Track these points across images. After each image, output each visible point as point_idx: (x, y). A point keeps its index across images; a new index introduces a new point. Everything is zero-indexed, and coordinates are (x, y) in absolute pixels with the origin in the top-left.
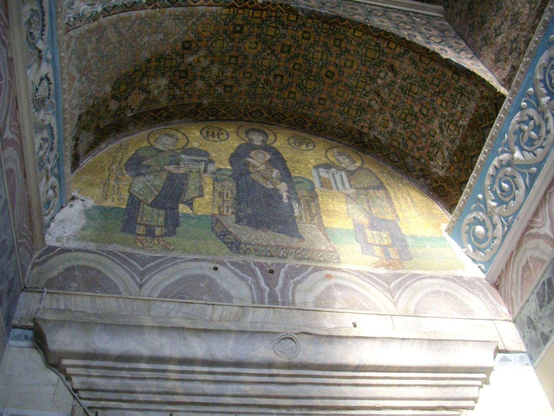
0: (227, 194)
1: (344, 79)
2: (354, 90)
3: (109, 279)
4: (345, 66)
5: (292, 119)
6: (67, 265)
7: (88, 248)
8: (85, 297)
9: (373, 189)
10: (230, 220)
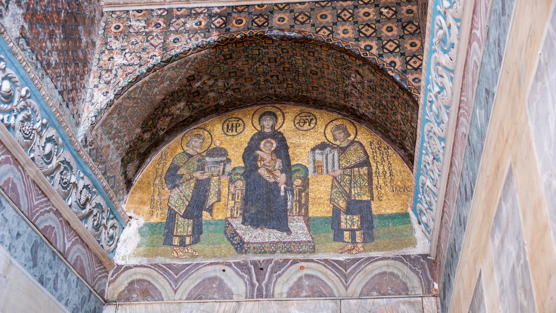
0: (238, 193)
1: (326, 75)
2: (336, 82)
3: (156, 289)
4: (323, 67)
5: (297, 99)
6: (130, 280)
7: (142, 263)
8: (141, 305)
9: (358, 167)
10: (237, 223)
